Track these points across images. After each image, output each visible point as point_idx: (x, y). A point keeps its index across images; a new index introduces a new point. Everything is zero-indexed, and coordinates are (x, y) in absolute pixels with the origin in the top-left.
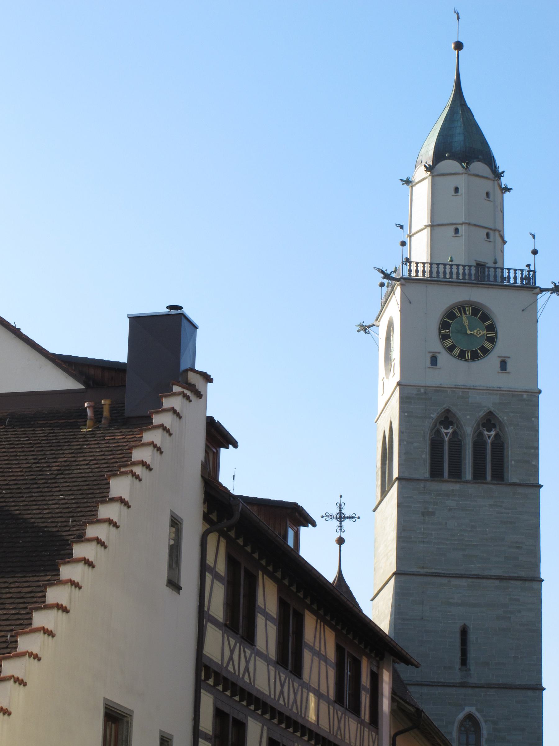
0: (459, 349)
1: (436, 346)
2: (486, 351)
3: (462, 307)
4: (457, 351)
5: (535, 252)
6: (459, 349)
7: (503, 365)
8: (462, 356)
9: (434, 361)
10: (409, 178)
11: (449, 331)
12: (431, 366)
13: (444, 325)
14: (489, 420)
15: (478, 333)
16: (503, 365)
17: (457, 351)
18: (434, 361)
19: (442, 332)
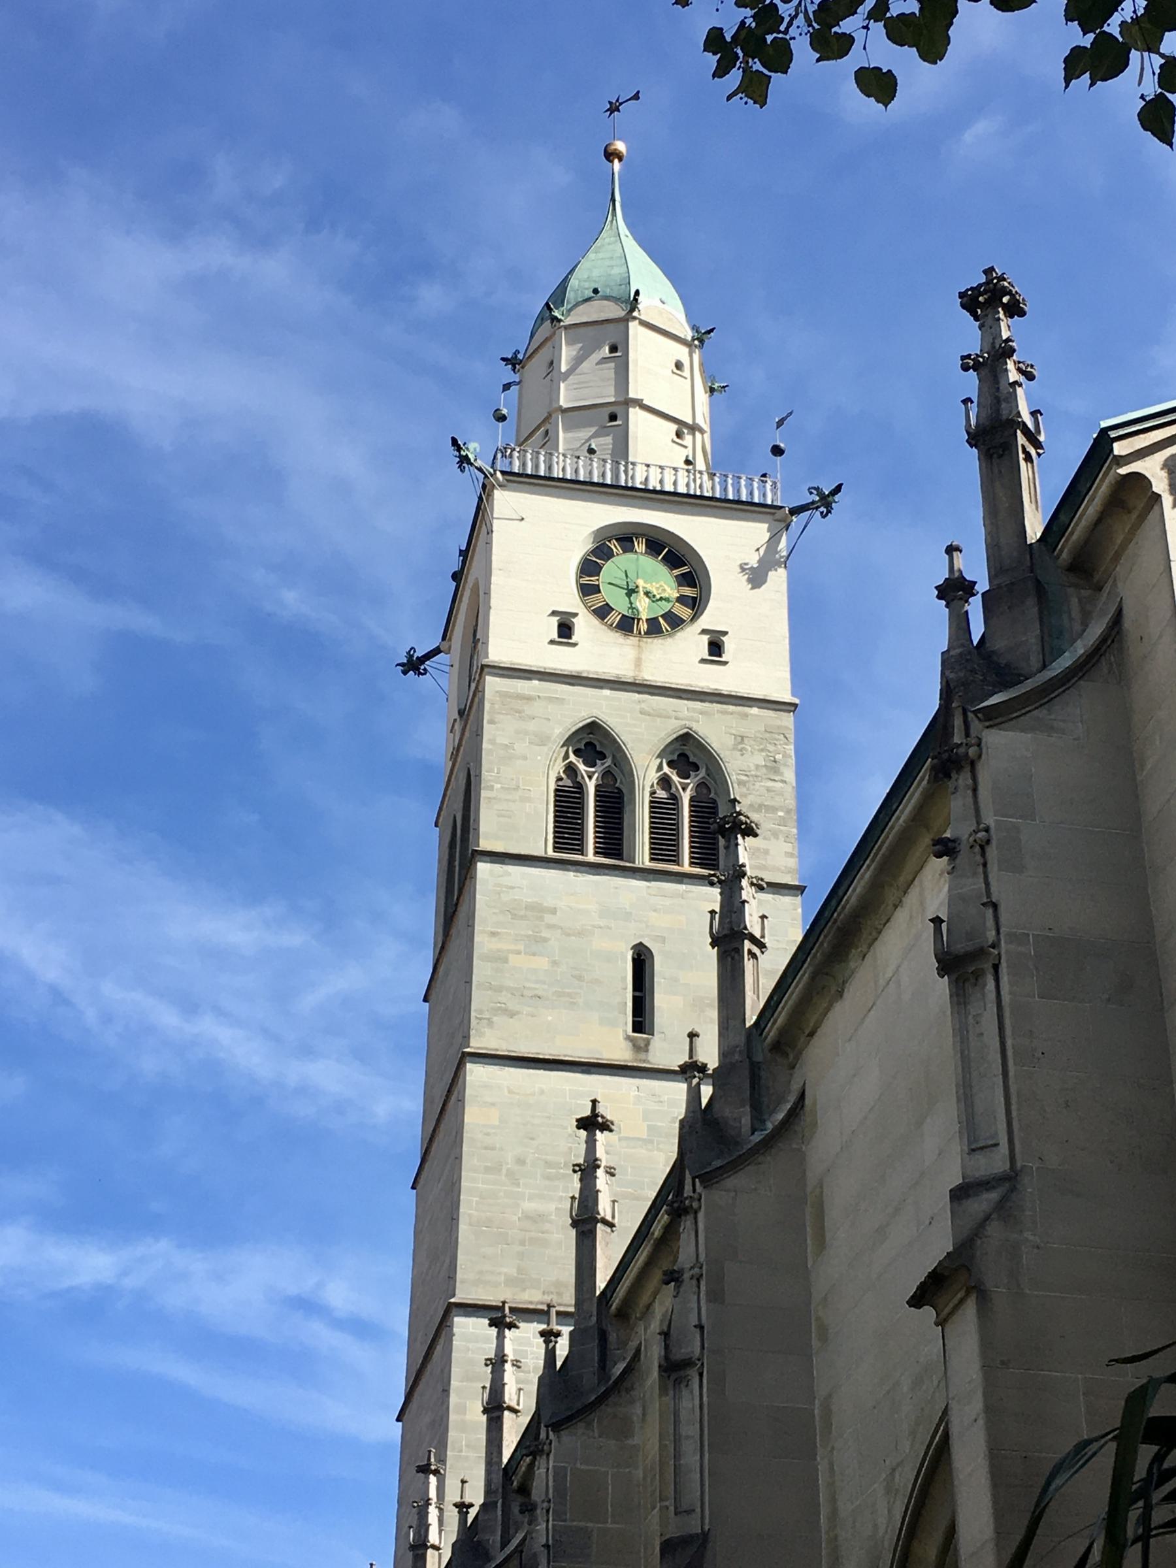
0: (620, 613)
1: (571, 601)
2: (675, 622)
3: (626, 537)
4: (614, 618)
6: (620, 613)
7: (716, 648)
9: (565, 630)
10: (519, 353)
11: (598, 580)
12: (560, 636)
13: (589, 567)
14: (683, 756)
15: (660, 591)
16: (716, 648)
17: (614, 618)
18: (565, 630)
19: (585, 580)
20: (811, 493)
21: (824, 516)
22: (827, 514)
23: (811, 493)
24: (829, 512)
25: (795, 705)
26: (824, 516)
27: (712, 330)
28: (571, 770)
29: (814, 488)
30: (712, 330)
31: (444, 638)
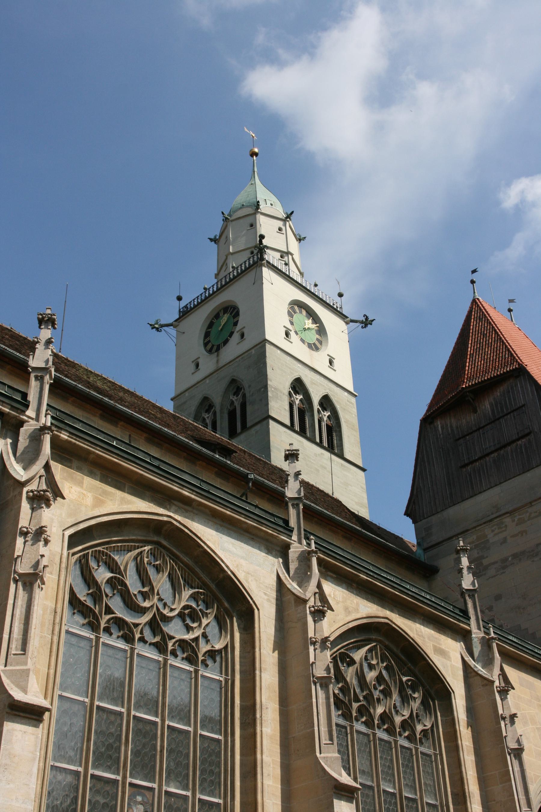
3: (301, 305)
5: (341, 295)
7: (331, 362)
8: (303, 341)
9: (287, 334)
16: (331, 362)
20: (364, 316)
21: (362, 327)
22: (364, 328)
23: (364, 316)
24: (365, 327)
25: (356, 396)
26: (362, 327)
27: (305, 238)
28: (290, 393)
29: (366, 316)
30: (305, 238)
31: (176, 321)
